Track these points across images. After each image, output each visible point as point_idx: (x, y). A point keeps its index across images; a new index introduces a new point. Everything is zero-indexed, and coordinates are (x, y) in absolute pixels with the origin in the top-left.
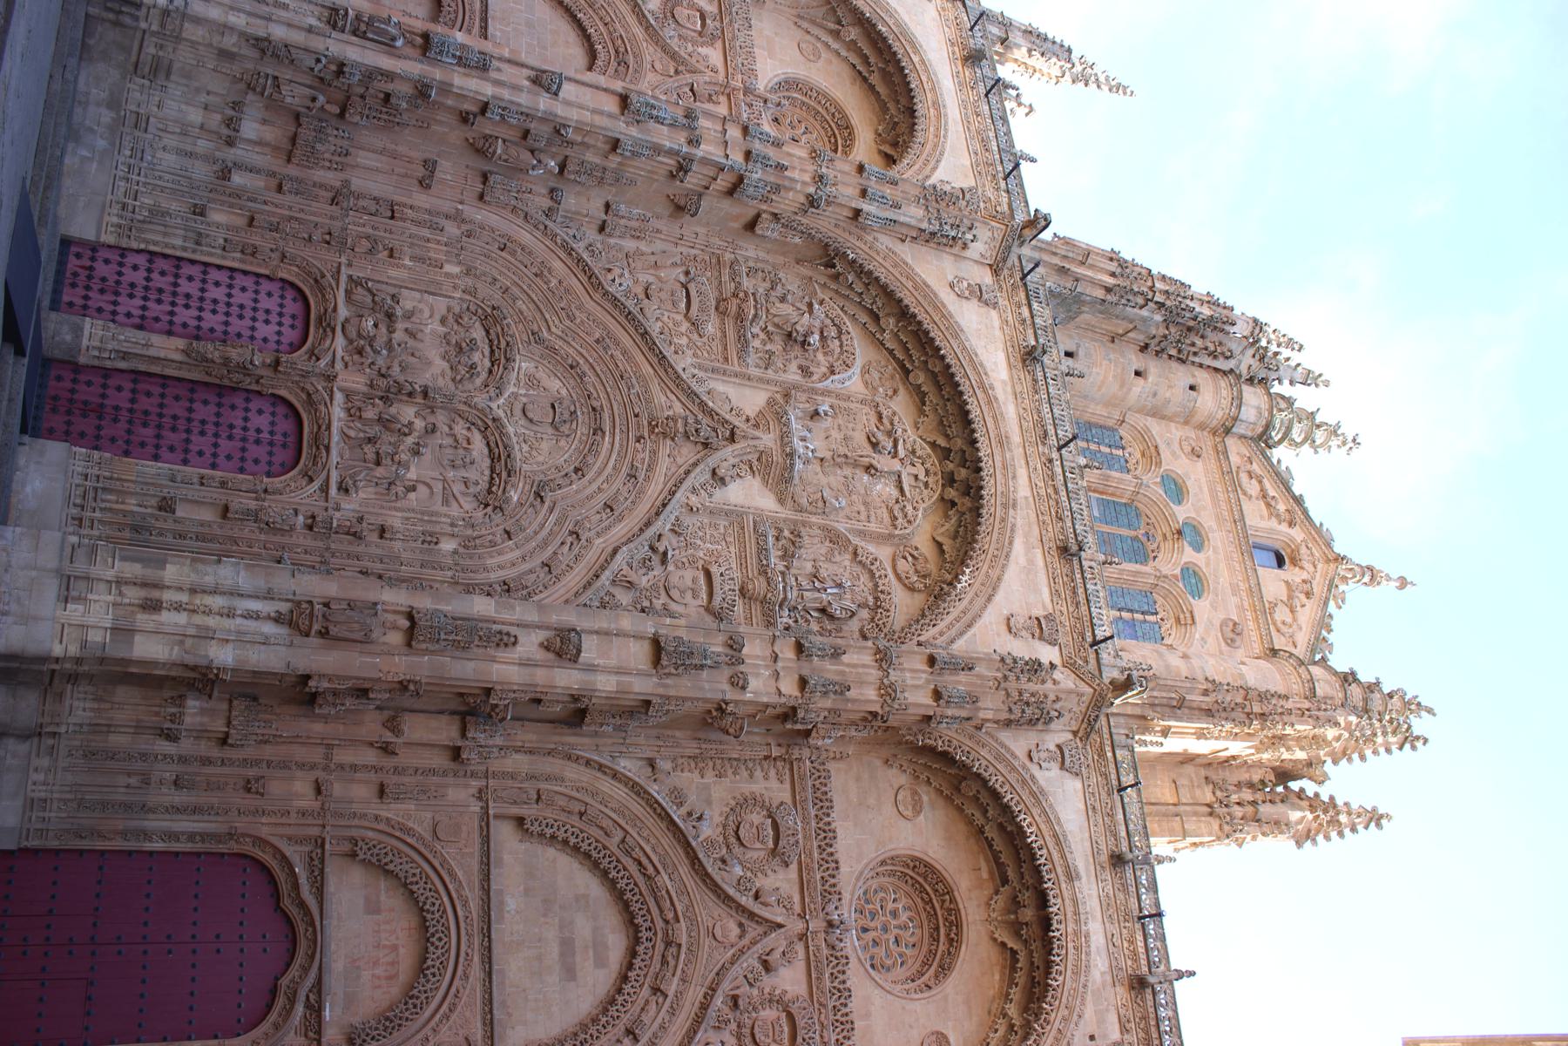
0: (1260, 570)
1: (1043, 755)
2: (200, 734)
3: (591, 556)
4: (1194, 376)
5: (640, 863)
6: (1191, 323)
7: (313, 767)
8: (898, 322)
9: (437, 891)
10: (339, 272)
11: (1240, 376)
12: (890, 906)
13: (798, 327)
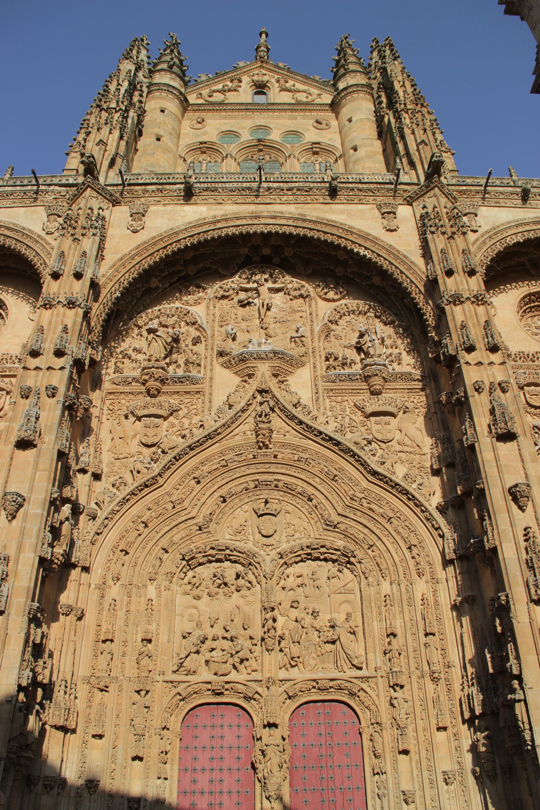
4: (155, 109)
10: (172, 682)
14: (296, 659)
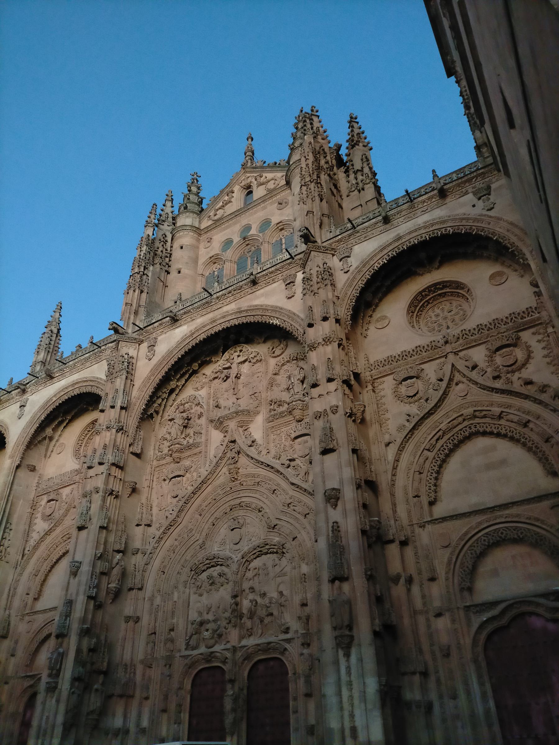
0: (255, 199)
1: (345, 266)
2: (424, 689)
3: (298, 495)
5: (438, 439)
6: (152, 254)
7: (428, 620)
8: (172, 380)
9: (477, 540)
11: (173, 229)
12: (434, 318)
13: (180, 423)
14: (250, 630)
